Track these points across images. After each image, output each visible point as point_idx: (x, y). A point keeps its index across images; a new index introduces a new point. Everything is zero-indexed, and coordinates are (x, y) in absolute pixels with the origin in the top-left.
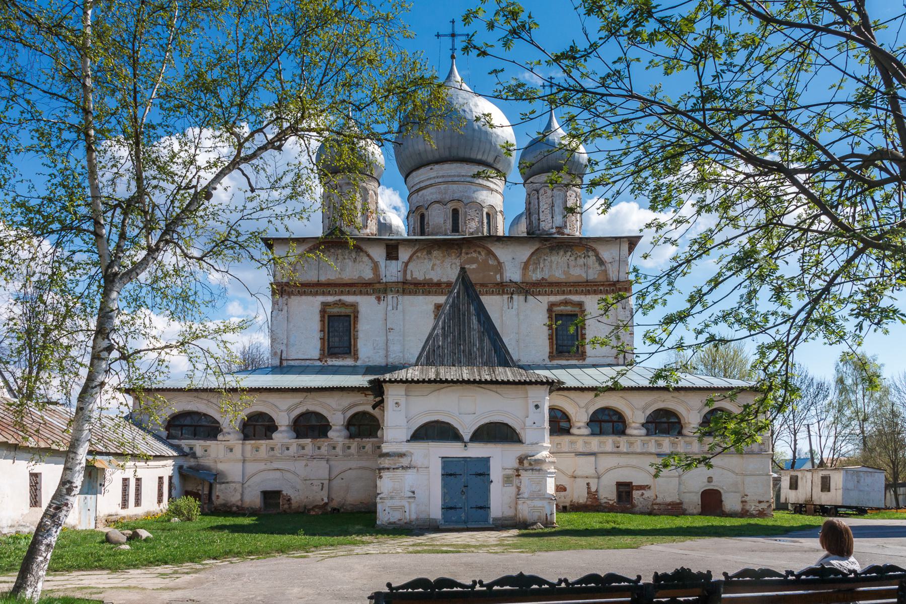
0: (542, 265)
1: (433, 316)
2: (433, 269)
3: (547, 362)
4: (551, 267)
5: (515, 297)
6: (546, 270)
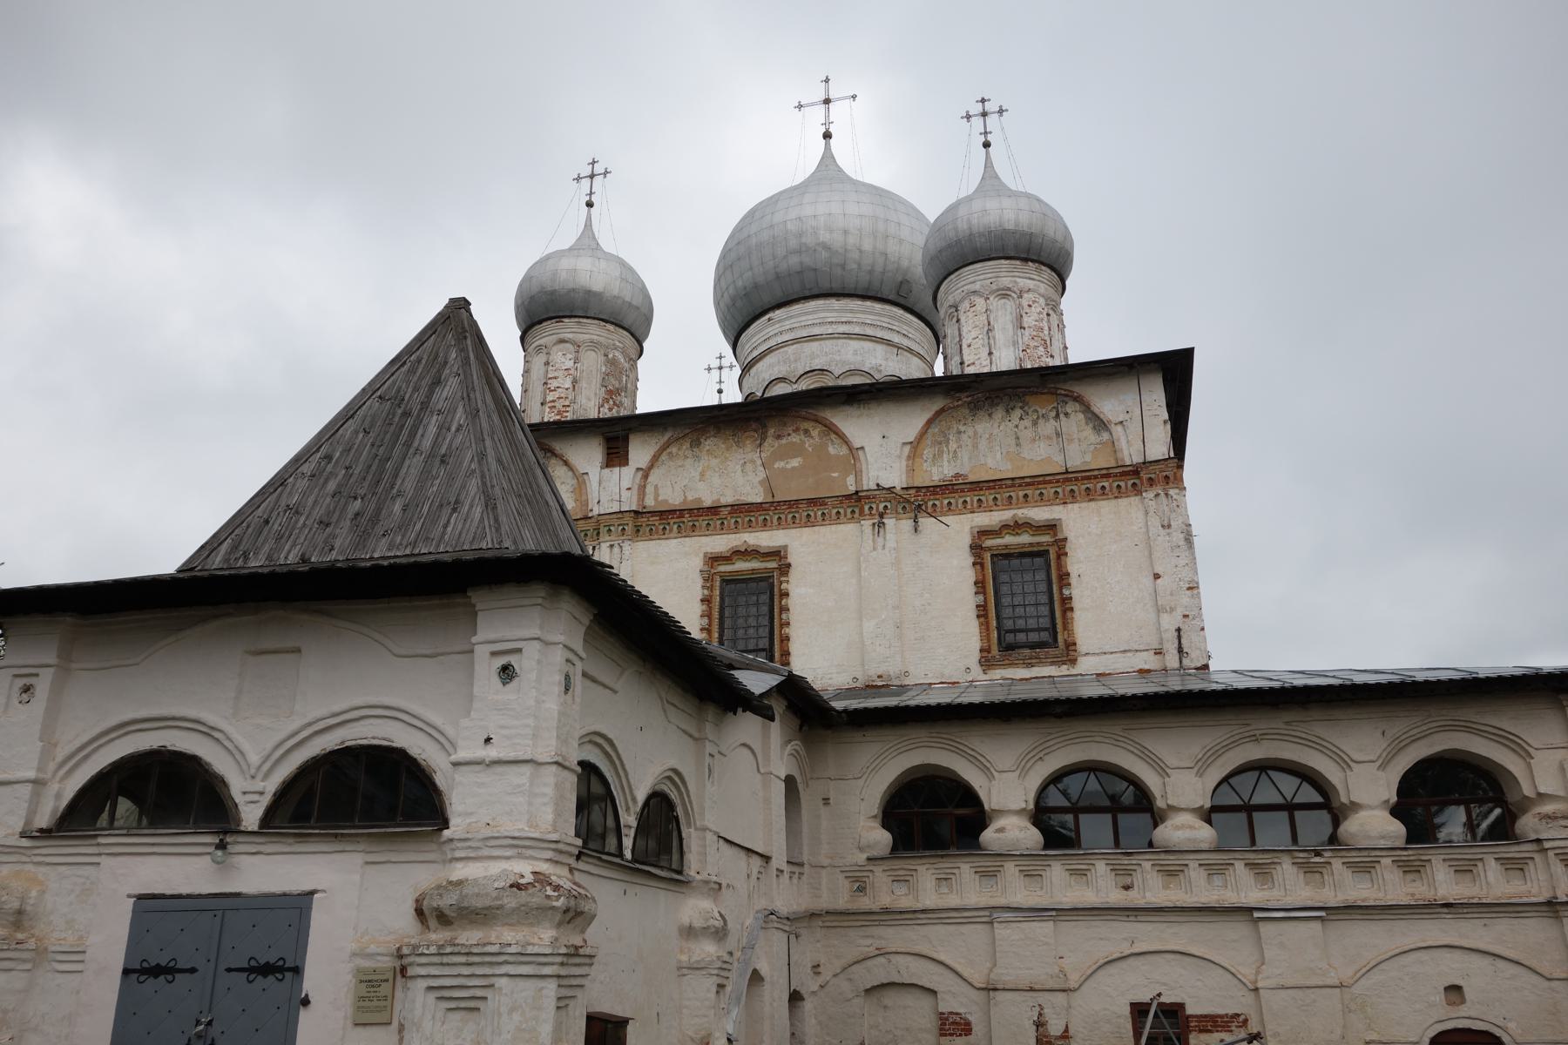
0: (953, 445)
1: (699, 582)
2: (702, 475)
3: (977, 672)
4: (975, 446)
5: (889, 522)
6: (964, 455)
